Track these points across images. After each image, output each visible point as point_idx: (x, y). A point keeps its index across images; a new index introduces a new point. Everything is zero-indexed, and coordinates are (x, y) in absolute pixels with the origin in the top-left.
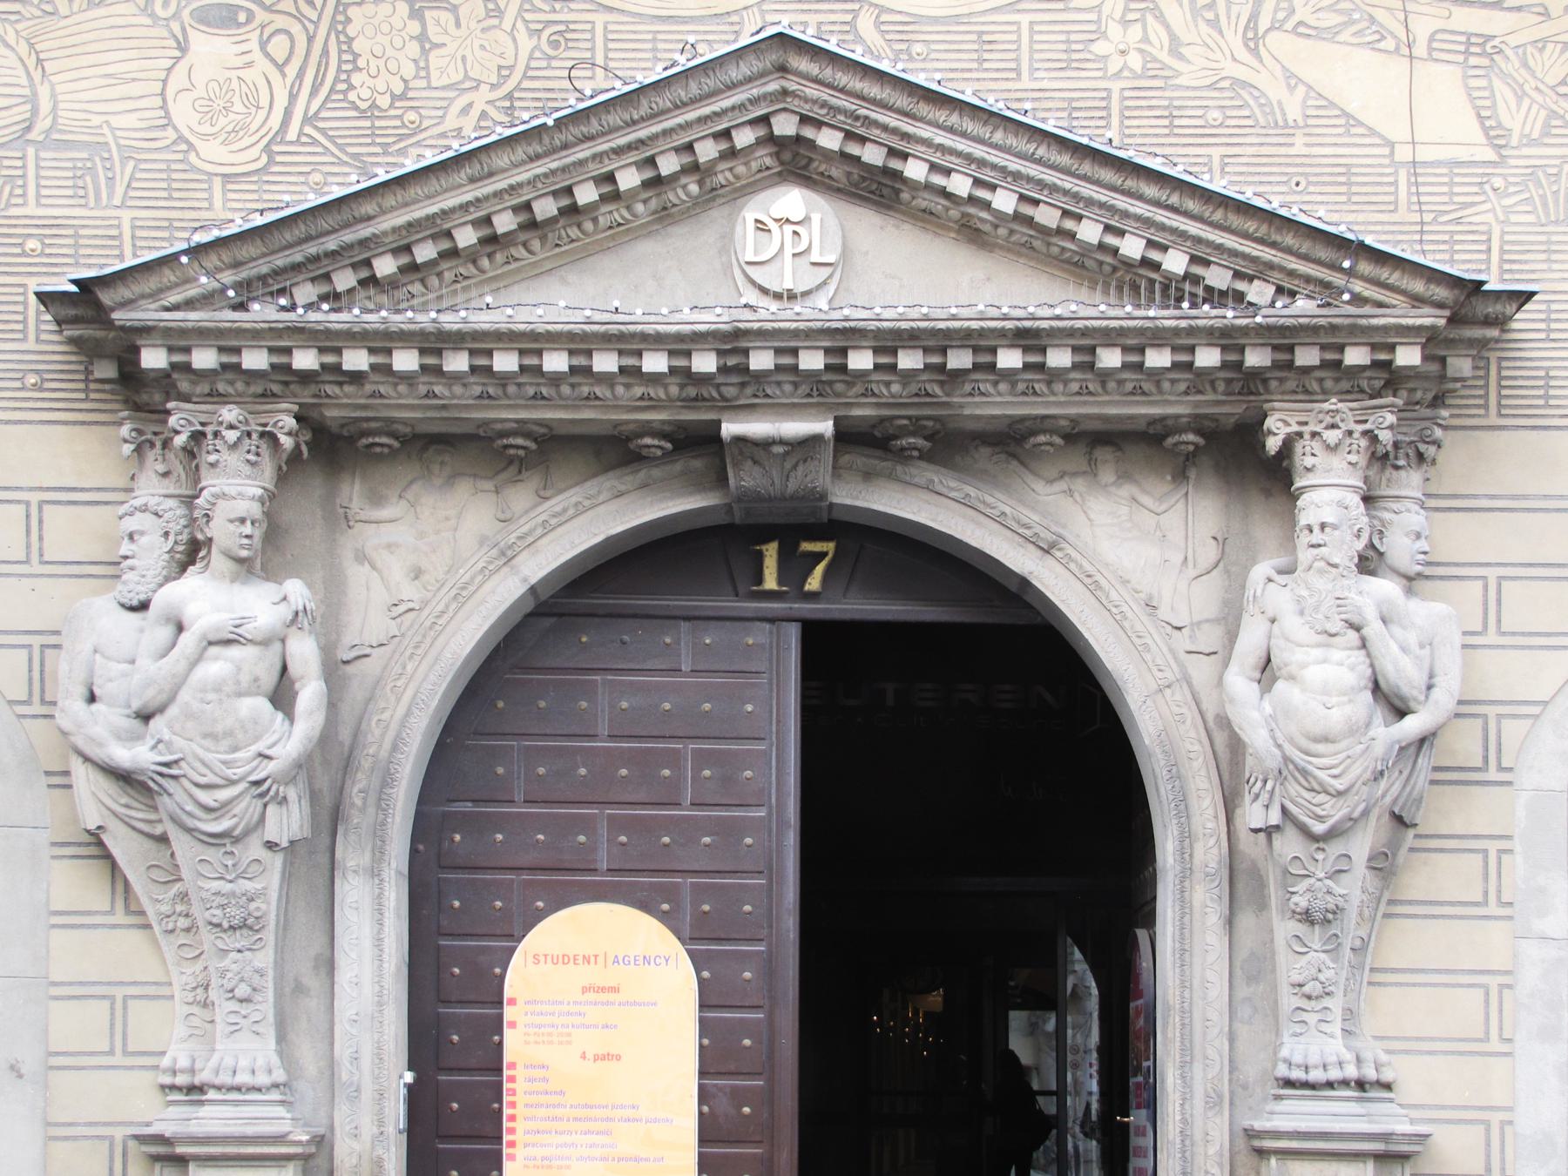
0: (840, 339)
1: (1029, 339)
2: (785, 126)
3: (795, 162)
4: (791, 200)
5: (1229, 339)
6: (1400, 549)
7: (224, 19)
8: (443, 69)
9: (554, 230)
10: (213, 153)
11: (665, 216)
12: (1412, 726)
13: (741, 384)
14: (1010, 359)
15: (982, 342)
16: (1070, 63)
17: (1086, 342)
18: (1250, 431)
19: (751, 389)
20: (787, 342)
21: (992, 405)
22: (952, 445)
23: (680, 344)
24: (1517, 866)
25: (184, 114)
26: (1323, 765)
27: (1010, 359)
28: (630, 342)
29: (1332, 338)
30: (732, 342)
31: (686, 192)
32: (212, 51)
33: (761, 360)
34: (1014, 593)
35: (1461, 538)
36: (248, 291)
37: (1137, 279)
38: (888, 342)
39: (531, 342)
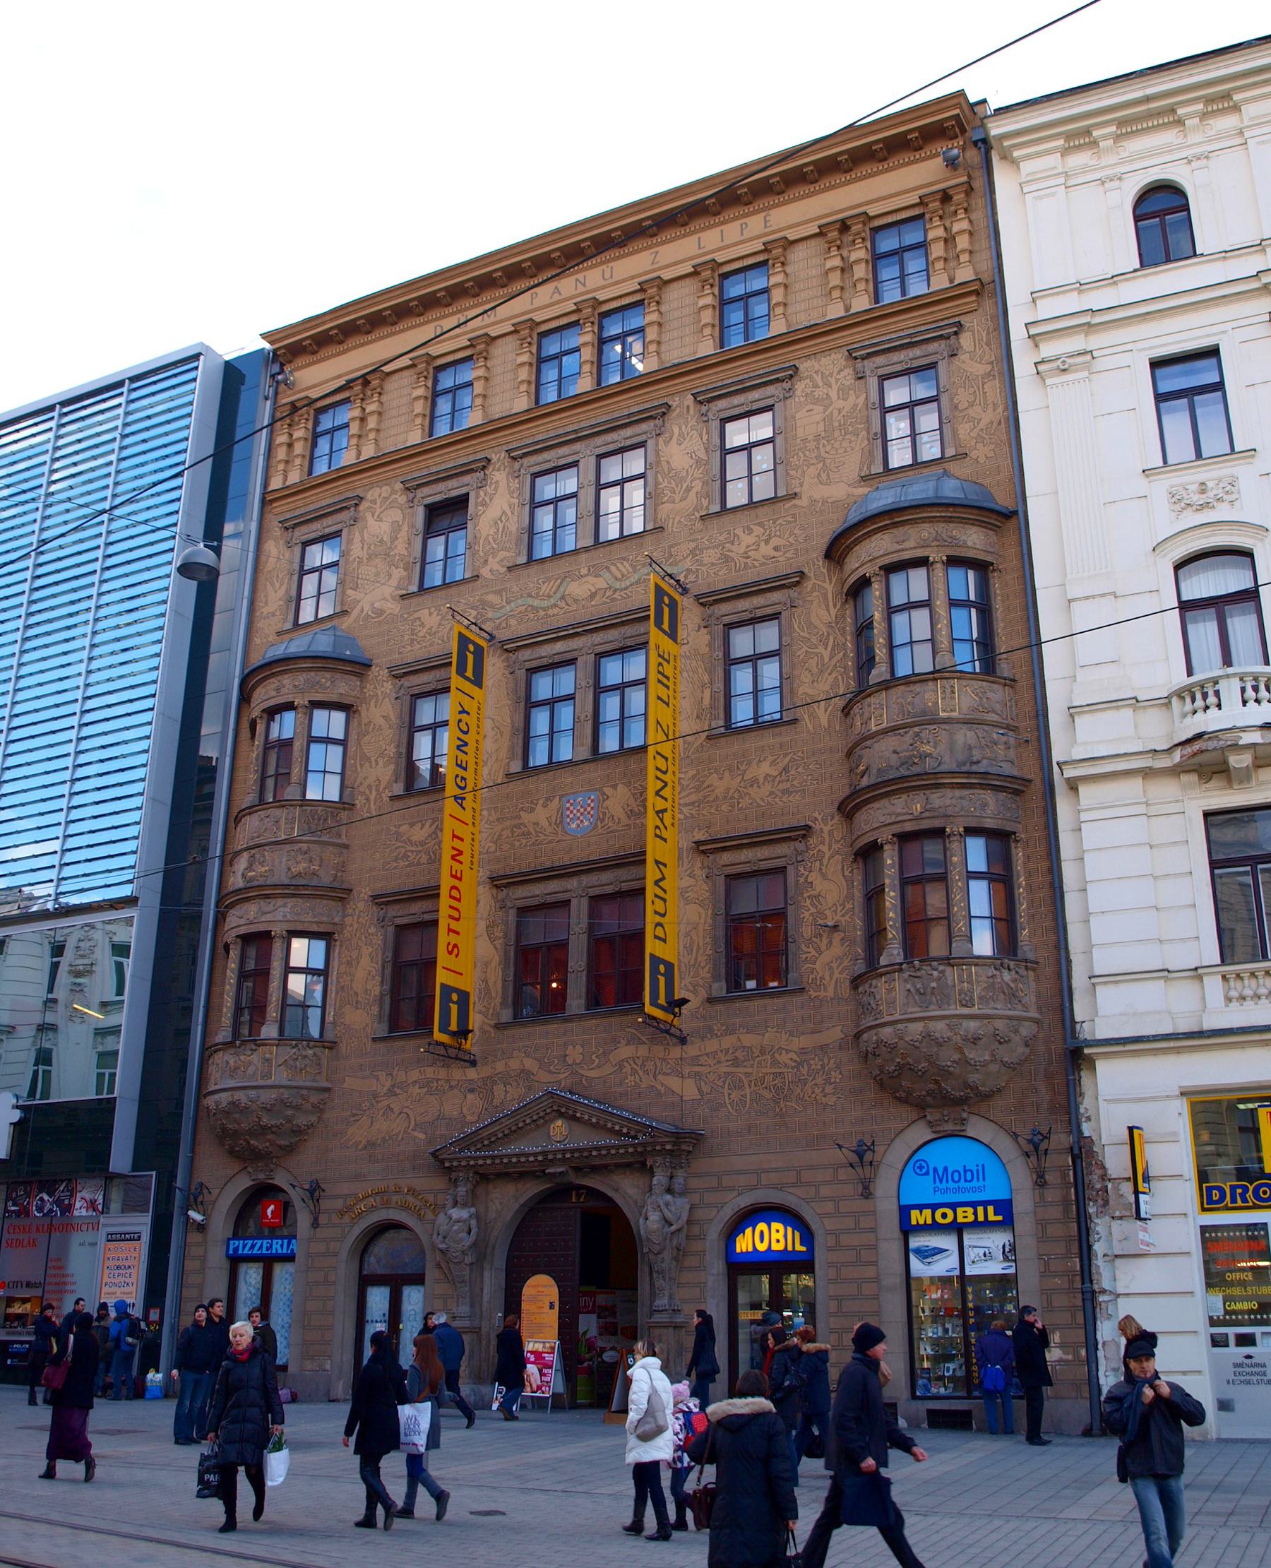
0: (564, 1151)
1: (598, 1149)
2: (555, 1108)
3: (561, 1115)
4: (559, 1123)
5: (634, 1145)
6: (677, 1187)
7: (472, 1091)
8: (509, 1097)
9: (514, 1133)
10: (469, 1118)
11: (538, 1126)
12: (673, 1228)
13: (548, 1162)
14: (594, 1153)
15: (590, 1150)
16: (621, 1085)
17: (608, 1148)
18: (644, 1164)
19: (553, 1162)
20: (555, 1152)
21: (598, 1162)
22: (596, 1169)
23: (535, 1155)
24: (707, 1257)
25: (465, 1110)
26: (654, 1238)
27: (594, 1153)
28: (528, 1155)
29: (654, 1144)
30: (544, 1153)
31: (541, 1122)
32: (470, 1096)
33: (550, 1157)
34: (610, 1200)
35: (694, 1183)
36: (461, 1150)
37: (619, 1133)
38: (572, 1151)
39: (509, 1156)
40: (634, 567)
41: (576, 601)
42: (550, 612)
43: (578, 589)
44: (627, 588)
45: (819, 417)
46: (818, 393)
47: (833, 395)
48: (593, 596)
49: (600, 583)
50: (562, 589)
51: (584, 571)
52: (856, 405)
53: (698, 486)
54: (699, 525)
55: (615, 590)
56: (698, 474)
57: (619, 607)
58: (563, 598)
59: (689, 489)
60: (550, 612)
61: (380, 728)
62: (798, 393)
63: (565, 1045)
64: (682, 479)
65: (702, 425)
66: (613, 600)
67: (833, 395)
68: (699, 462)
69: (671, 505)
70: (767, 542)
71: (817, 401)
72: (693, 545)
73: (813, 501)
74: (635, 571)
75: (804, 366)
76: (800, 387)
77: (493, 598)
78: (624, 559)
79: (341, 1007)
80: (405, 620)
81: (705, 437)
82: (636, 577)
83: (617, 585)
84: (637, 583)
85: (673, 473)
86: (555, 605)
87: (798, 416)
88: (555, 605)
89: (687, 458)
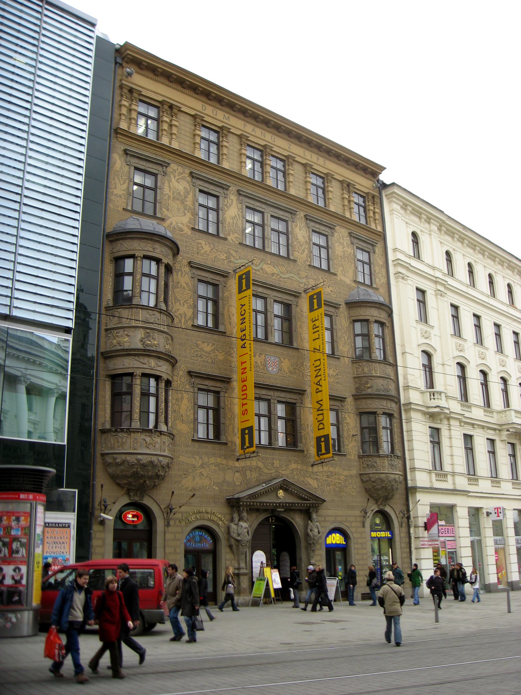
40: (287, 271)
41: (267, 273)
42: (257, 272)
43: (269, 269)
44: (284, 278)
45: (341, 250)
46: (341, 240)
47: (345, 244)
48: (273, 274)
49: (275, 271)
50: (261, 265)
51: (269, 262)
52: (351, 253)
53: (306, 252)
54: (307, 267)
55: (281, 277)
56: (307, 246)
57: (282, 285)
58: (262, 269)
59: (304, 251)
60: (257, 272)
61: (184, 288)
62: (335, 236)
63: (273, 459)
64: (301, 245)
65: (306, 228)
66: (280, 281)
67: (345, 244)
68: (306, 241)
69: (298, 254)
70: (329, 287)
71: (340, 243)
72: (306, 274)
73: (341, 280)
74: (287, 273)
75: (337, 228)
76: (336, 234)
77: (234, 254)
78: (283, 266)
79: (175, 420)
80: (194, 240)
81: (308, 234)
82: (287, 276)
83: (281, 275)
84: (288, 278)
85: (298, 241)
86: (258, 271)
87: (336, 245)
88: (258, 271)
89: (302, 238)
